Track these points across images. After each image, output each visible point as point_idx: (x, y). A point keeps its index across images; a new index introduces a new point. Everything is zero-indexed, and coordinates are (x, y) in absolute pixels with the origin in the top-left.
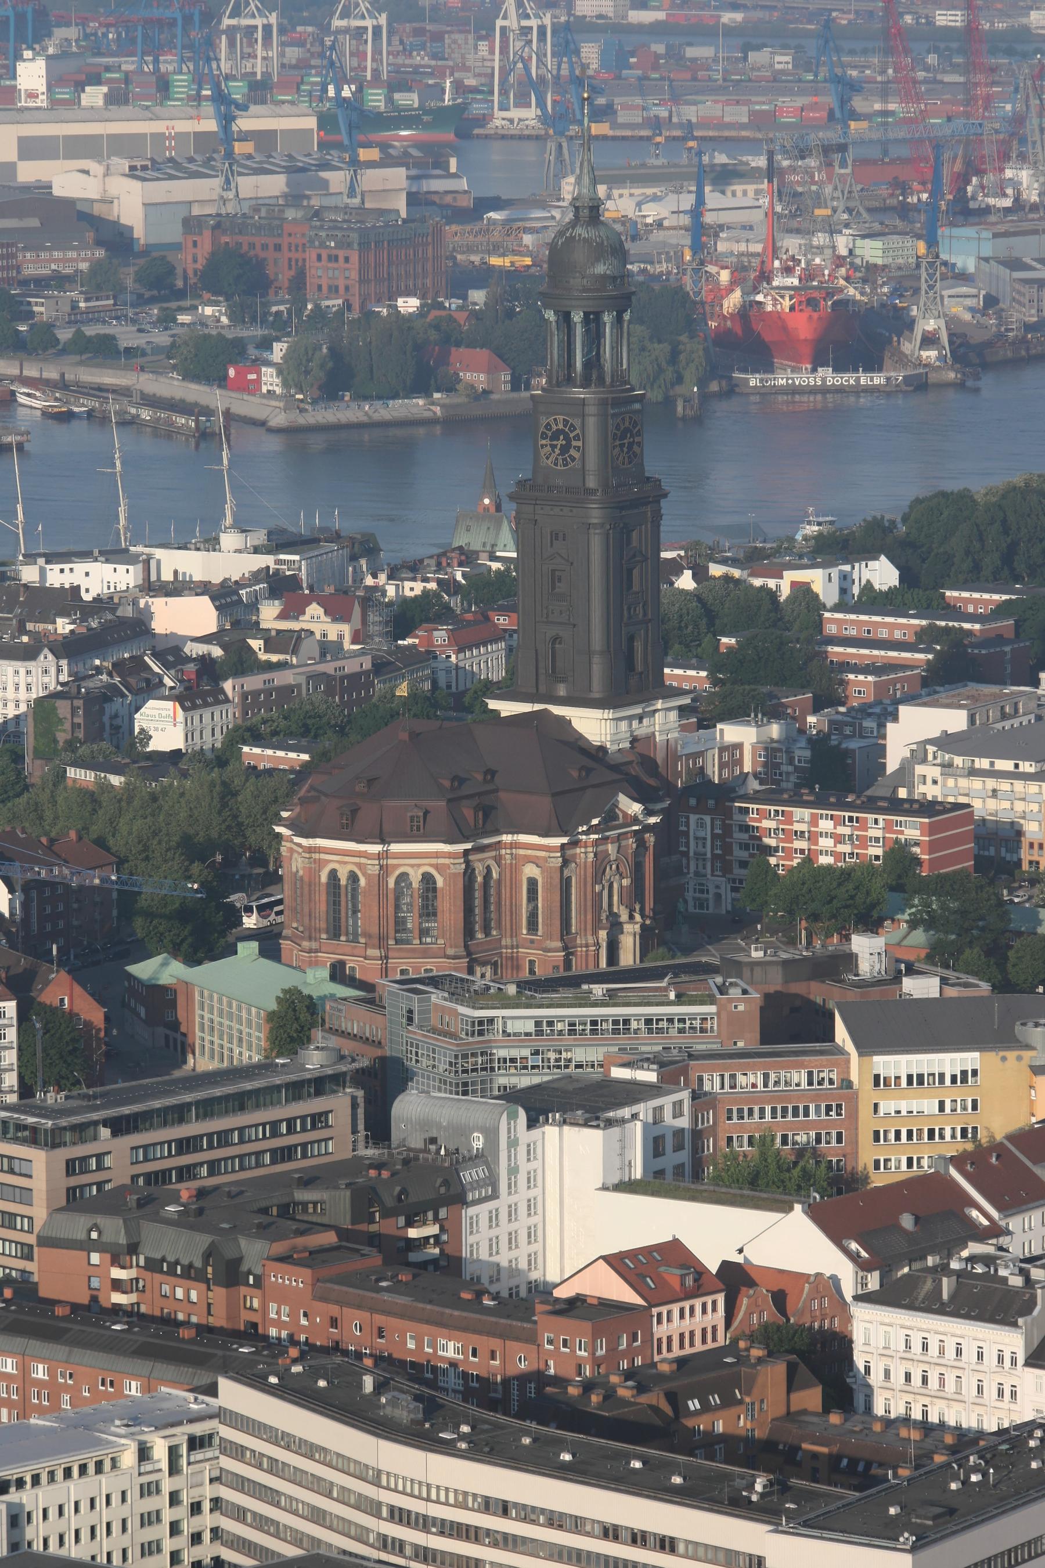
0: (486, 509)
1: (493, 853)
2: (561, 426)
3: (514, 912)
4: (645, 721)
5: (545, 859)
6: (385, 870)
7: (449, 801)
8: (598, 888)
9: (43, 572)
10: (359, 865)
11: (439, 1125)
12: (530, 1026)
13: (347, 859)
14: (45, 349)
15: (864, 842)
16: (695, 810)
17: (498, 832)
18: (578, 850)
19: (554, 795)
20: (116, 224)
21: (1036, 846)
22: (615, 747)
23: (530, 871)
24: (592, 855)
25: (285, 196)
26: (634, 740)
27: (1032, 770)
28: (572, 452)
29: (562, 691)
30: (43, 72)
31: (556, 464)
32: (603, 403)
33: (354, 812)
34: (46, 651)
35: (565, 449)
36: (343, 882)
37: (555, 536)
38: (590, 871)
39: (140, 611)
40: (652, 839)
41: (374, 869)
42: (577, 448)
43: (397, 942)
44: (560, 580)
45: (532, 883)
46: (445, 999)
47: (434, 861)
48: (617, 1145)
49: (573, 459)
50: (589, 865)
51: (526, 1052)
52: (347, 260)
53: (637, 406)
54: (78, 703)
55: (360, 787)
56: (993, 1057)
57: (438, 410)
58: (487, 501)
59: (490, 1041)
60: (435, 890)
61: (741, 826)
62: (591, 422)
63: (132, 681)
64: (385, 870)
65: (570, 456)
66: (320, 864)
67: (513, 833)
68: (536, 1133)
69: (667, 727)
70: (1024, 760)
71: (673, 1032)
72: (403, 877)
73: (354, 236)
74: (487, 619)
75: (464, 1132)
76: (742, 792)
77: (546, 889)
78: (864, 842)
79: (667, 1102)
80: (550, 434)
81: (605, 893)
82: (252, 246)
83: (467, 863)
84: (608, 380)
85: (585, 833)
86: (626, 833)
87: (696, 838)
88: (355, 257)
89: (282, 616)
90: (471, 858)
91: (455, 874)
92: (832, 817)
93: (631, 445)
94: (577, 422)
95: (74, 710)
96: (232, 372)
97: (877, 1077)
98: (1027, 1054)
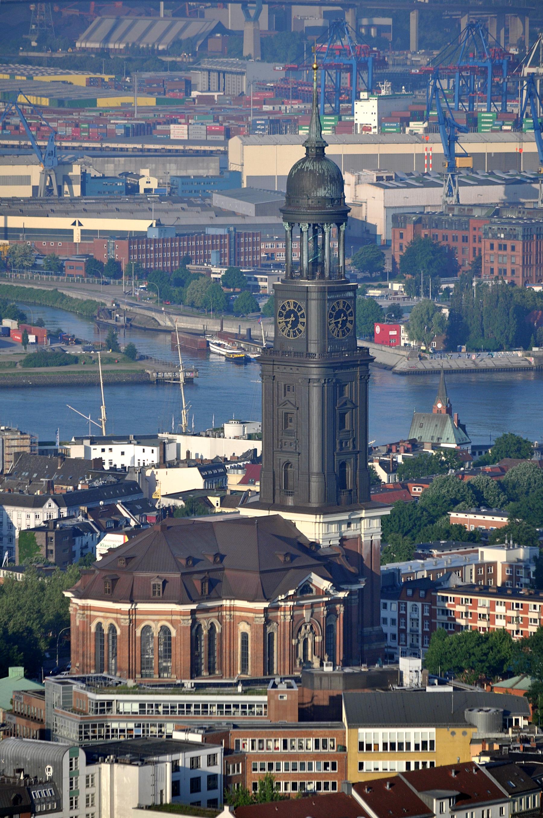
0: (439, 411)
1: (216, 614)
2: (292, 308)
3: (232, 658)
4: (353, 525)
5: (253, 619)
6: (133, 623)
7: (183, 574)
8: (294, 642)
9: (87, 451)
10: (117, 620)
11: (25, 761)
12: (136, 707)
13: (108, 615)
14: (247, 312)
15: (526, 622)
16: (411, 599)
17: (220, 598)
18: (279, 613)
19: (261, 572)
20: (364, 222)
22: (327, 544)
23: (243, 627)
24: (289, 617)
25: (504, 202)
26: (343, 540)
28: (300, 326)
29: (290, 502)
30: (375, 110)
31: (289, 335)
32: (322, 291)
33: (115, 581)
34: (50, 501)
35: (295, 324)
36: (106, 632)
37: (287, 388)
38: (287, 629)
39: (146, 479)
40: (342, 609)
41: (126, 623)
44: (291, 421)
45: (245, 636)
46: (82, 688)
47: (169, 617)
48: (151, 779)
49: (300, 332)
50: (287, 624)
51: (131, 726)
52: (513, 248)
53: (350, 294)
54: (52, 534)
55: (121, 564)
56: (445, 732)
57: (532, 360)
58: (440, 406)
59: (106, 717)
60: (170, 638)
61: (443, 611)
62: (314, 305)
63: (103, 521)
64: (133, 623)
65: (298, 329)
66: (91, 618)
67: (230, 599)
68: (93, 768)
69: (371, 531)
71: (239, 714)
72: (147, 628)
73: (519, 230)
74: (407, 488)
75: (40, 765)
76: (446, 586)
77: (255, 641)
78: (526, 622)
79: (203, 754)
81: (301, 646)
82: (445, 238)
83: (194, 620)
84: (327, 274)
85: (285, 600)
86: (319, 603)
87: (412, 619)
88: (519, 246)
89: (243, 482)
90: (198, 616)
91: (184, 627)
93: (344, 323)
94: (303, 306)
95: (48, 540)
96: (378, 330)
97: (361, 744)
98: (470, 731)
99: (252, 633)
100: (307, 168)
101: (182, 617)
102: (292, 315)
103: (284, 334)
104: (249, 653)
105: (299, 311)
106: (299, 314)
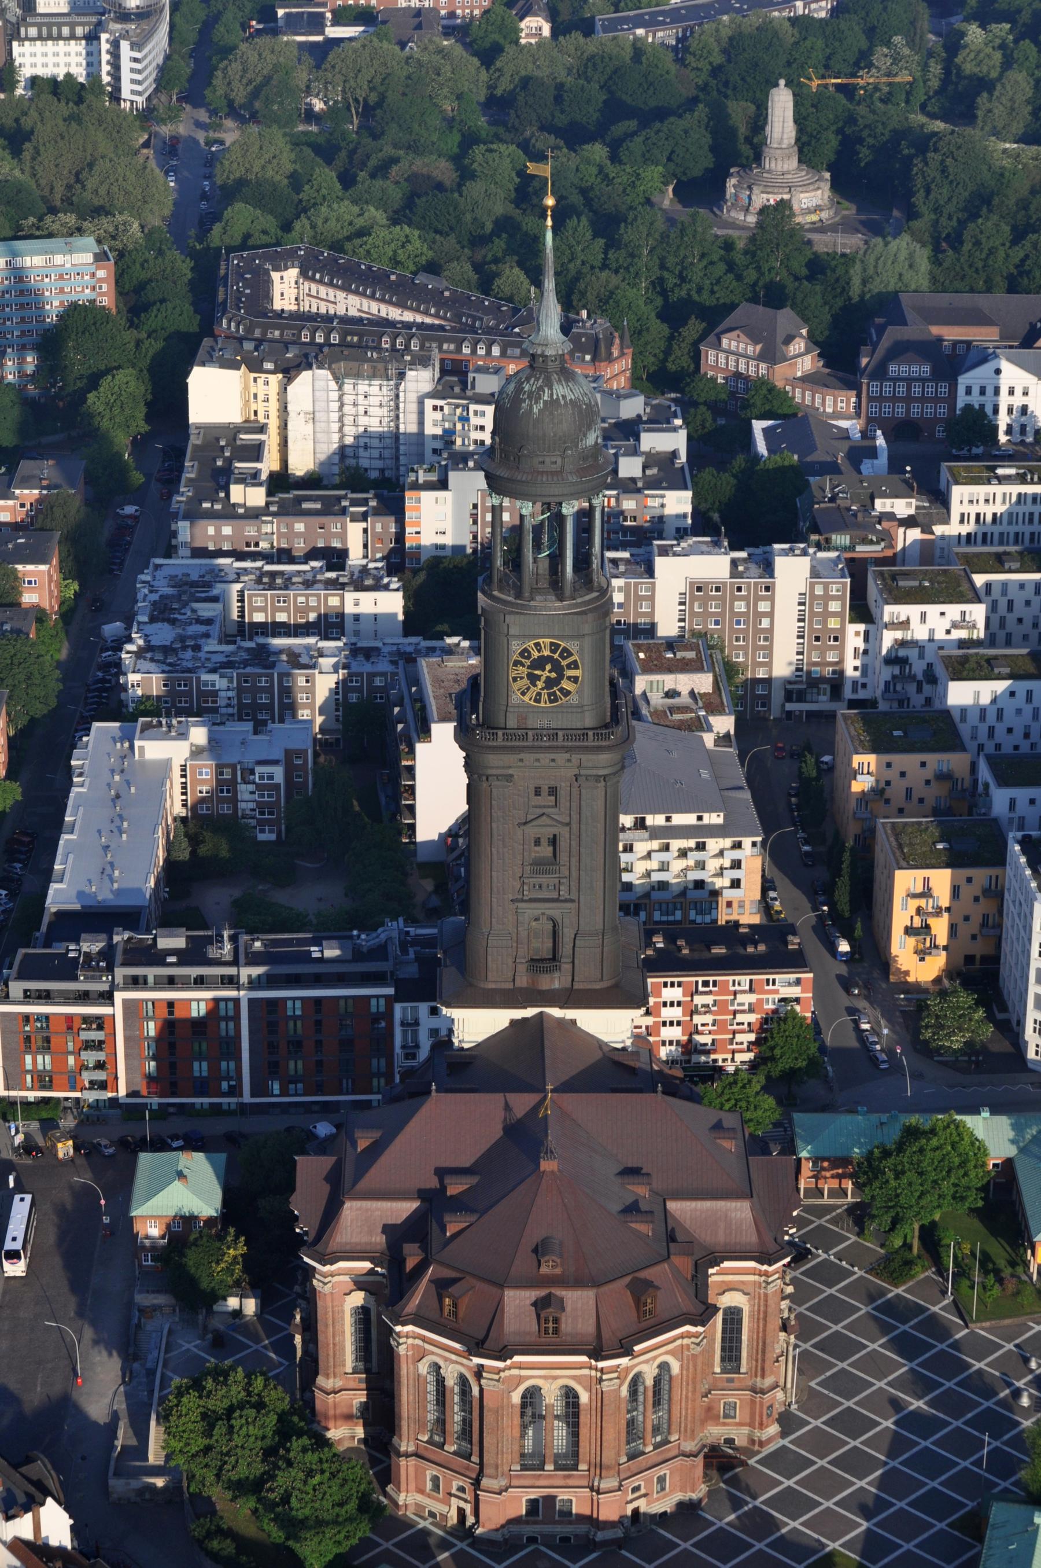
2: (546, 653)
21: (735, 905)
27: (720, 820)
28: (565, 684)
29: (556, 982)
42: (575, 680)
43: (631, 1457)
49: (567, 693)
62: (588, 642)
65: (562, 690)
70: (710, 810)
80: (528, 662)
92: (680, 985)
94: (573, 646)
99: (752, 1306)
100: (564, 397)
101: (693, 1340)
102: (548, 667)
103: (526, 698)
104: (745, 1337)
105: (564, 658)
106: (564, 663)
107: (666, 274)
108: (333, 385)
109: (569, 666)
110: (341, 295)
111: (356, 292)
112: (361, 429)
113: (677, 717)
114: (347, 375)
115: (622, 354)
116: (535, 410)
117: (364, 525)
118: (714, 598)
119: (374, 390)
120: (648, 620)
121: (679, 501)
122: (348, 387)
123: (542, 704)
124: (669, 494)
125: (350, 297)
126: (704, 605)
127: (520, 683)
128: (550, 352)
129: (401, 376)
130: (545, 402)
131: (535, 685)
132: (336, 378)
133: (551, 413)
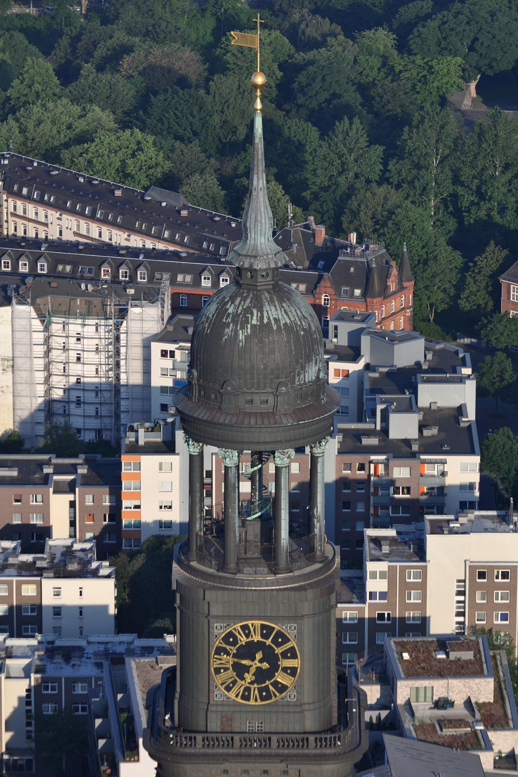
2: (257, 638)
28: (280, 678)
31: (245, 697)
42: (293, 672)
49: (282, 688)
62: (308, 624)
65: (276, 684)
100: (277, 320)
102: (259, 656)
103: (232, 695)
105: (278, 645)
106: (278, 651)
107: (460, 190)
108: (37, 324)
109: (284, 655)
110: (53, 215)
111: (72, 212)
112: (73, 380)
113: (449, 732)
114: (56, 313)
115: (401, 288)
116: (241, 337)
117: (71, 497)
118: (501, 587)
119: (90, 331)
120: (418, 614)
121: (464, 468)
122: (56, 328)
123: (252, 702)
124: (450, 459)
125: (65, 217)
126: (488, 595)
127: (224, 675)
128: (259, 265)
129: (123, 313)
130: (253, 327)
131: (243, 678)
132: (41, 316)
133: (261, 341)
